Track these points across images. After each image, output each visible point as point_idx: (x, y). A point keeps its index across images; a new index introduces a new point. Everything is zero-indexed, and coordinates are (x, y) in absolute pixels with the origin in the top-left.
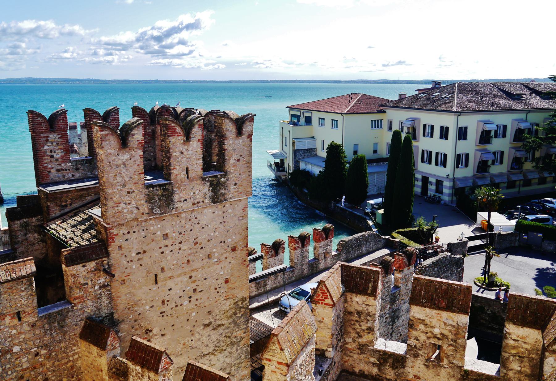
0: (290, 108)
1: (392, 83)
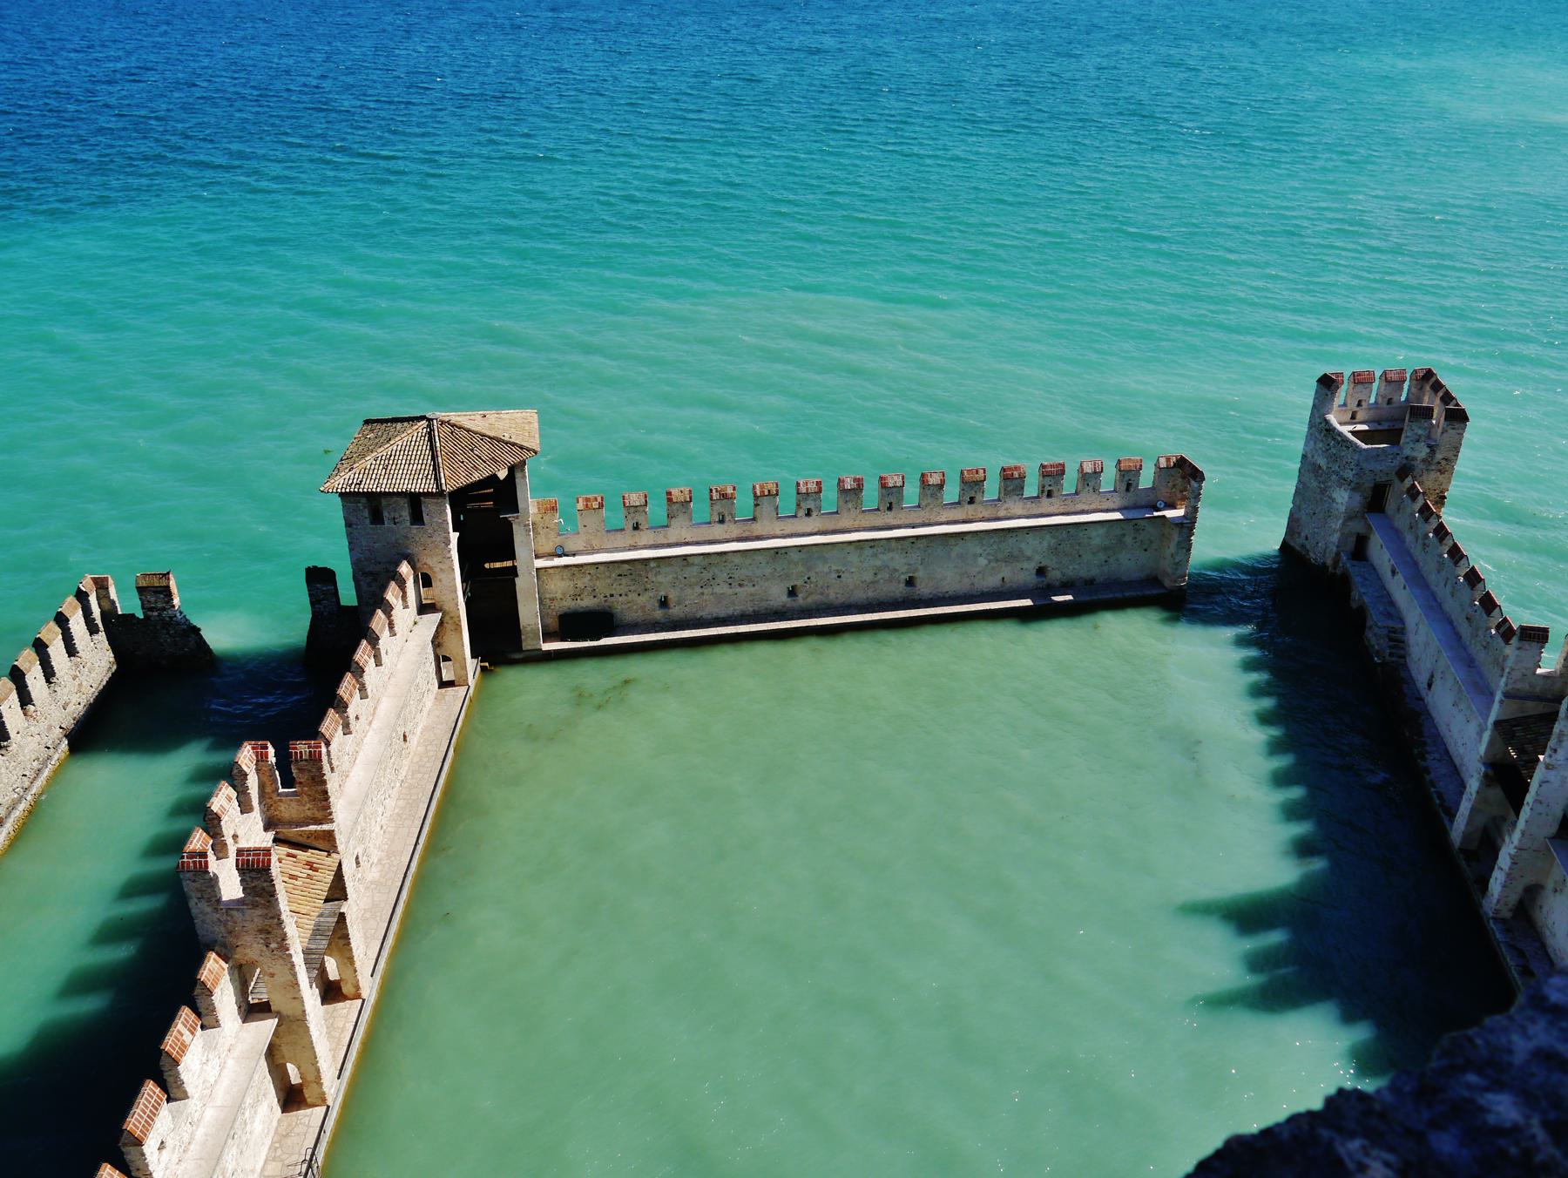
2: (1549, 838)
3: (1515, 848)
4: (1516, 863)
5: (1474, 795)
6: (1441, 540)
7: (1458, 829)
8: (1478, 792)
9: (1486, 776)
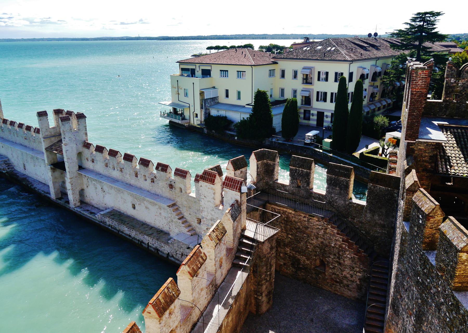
0: (181, 63)
1: (155, 39)
2: (78, 171)
3: (70, 179)
4: (72, 184)
5: (51, 177)
6: (6, 123)
7: (53, 196)
8: (52, 176)
9: (51, 168)
